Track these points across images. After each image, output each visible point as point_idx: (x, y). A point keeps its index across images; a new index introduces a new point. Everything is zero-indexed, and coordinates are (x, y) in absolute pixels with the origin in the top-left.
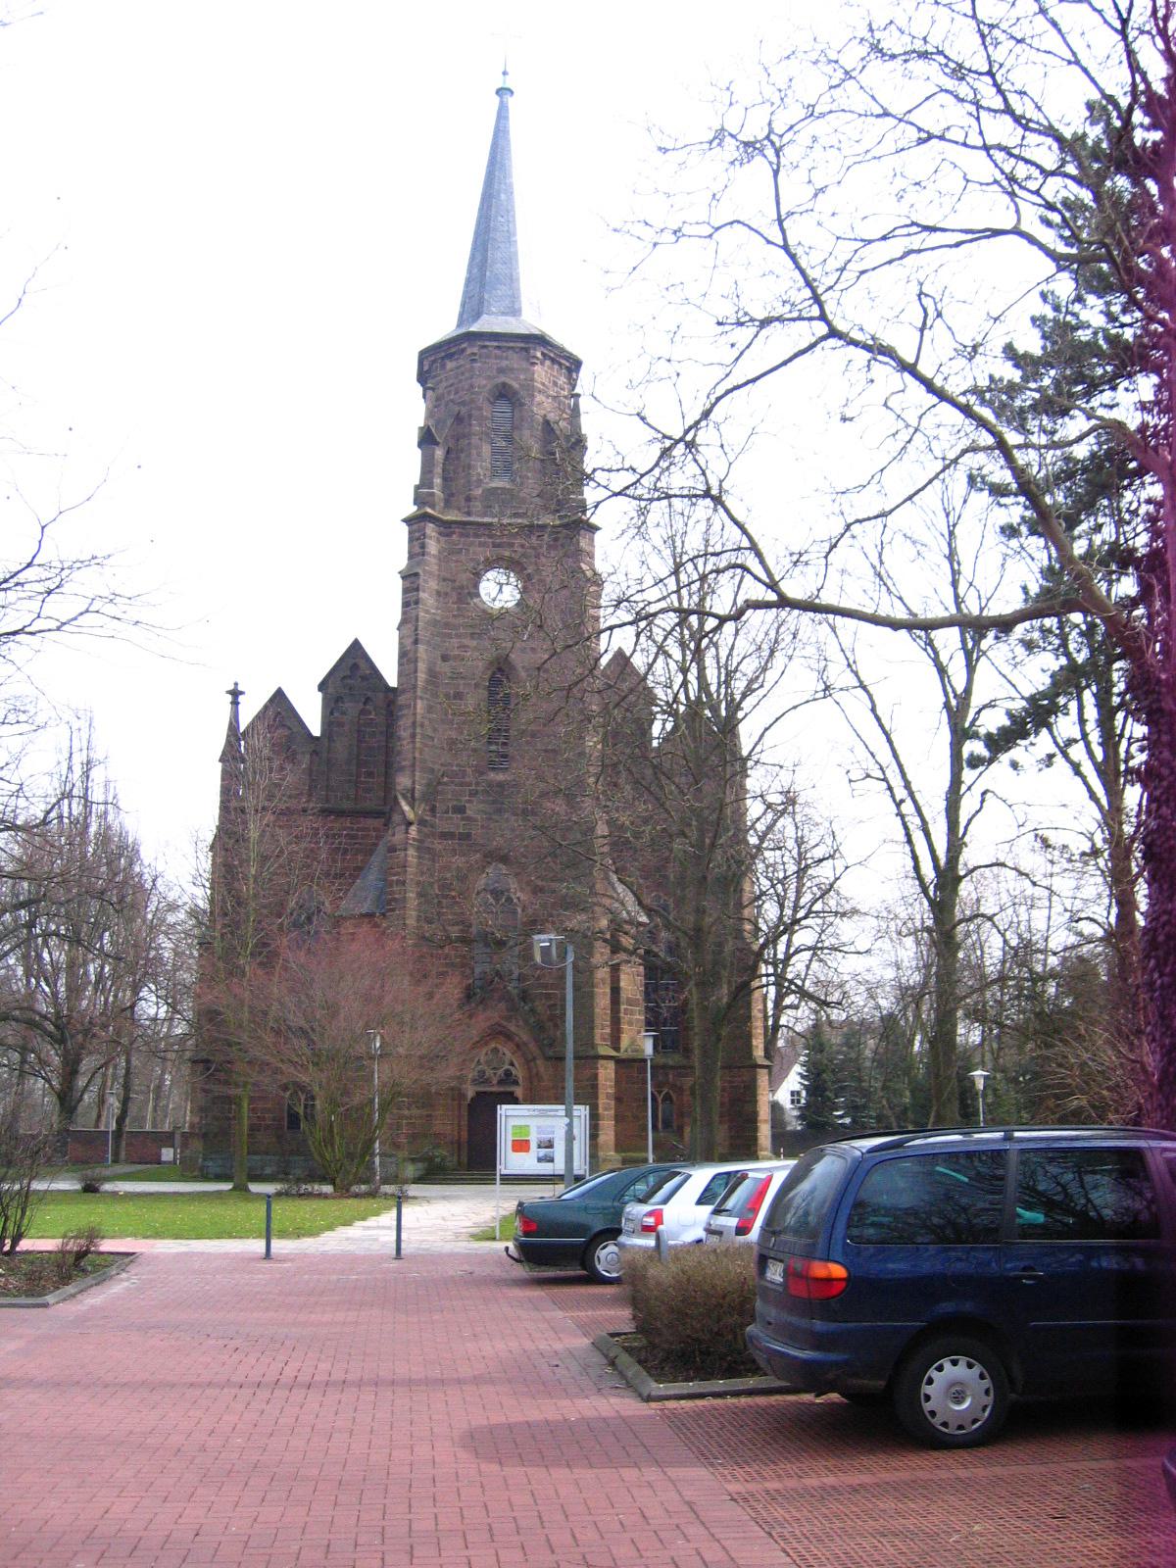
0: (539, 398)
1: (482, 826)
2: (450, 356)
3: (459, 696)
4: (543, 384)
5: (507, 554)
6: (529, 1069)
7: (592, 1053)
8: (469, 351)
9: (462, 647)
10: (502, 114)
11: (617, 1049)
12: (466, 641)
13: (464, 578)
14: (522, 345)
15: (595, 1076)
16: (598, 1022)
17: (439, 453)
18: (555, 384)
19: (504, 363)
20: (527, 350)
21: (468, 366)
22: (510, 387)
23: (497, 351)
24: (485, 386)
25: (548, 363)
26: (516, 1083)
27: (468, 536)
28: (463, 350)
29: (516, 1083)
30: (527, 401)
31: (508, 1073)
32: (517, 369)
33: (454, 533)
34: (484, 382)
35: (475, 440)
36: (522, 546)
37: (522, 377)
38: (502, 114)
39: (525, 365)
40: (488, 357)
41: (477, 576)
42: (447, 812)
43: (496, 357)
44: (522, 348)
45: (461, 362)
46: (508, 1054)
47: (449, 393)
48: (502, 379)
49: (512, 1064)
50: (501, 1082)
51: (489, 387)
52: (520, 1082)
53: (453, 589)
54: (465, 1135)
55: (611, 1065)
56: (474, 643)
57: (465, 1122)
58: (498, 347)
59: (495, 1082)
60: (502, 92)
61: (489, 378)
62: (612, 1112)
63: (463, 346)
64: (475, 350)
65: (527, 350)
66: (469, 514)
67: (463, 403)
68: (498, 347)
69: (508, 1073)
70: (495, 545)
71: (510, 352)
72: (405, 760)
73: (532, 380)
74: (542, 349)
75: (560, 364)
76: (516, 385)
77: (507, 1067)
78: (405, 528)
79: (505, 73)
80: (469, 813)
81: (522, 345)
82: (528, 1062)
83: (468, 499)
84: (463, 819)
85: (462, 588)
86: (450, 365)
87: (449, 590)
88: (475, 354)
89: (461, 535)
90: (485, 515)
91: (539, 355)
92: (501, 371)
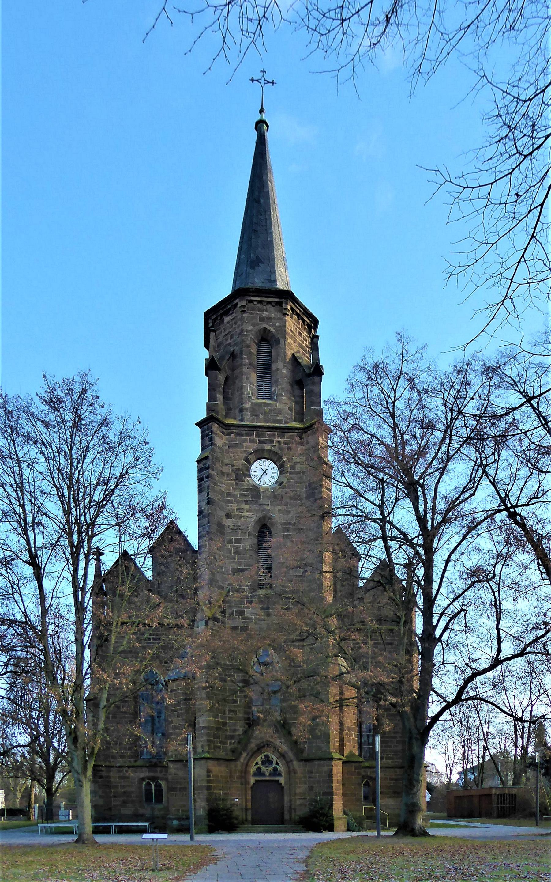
0: (289, 340)
1: (256, 623)
2: (227, 313)
3: (238, 541)
4: (291, 331)
5: (269, 447)
6: (289, 768)
7: (329, 757)
8: (240, 305)
9: (239, 509)
10: (261, 142)
11: (343, 755)
12: (243, 506)
13: (240, 463)
14: (277, 300)
15: (331, 770)
16: (332, 738)
17: (221, 378)
18: (300, 334)
19: (265, 314)
20: (280, 304)
21: (239, 317)
22: (269, 331)
23: (259, 305)
24: (251, 331)
25: (295, 317)
26: (280, 775)
27: (241, 435)
28: (237, 304)
29: (280, 775)
30: (282, 341)
31: (275, 769)
32: (274, 318)
33: (232, 433)
34: (250, 328)
35: (245, 369)
36: (279, 442)
37: (277, 324)
38: (261, 142)
39: (279, 315)
40: (253, 309)
41: (249, 463)
42: (232, 614)
43: (259, 310)
44: (277, 303)
45: (234, 315)
46: (275, 758)
47: (226, 340)
48: (264, 325)
49: (277, 764)
50: (270, 775)
52: (283, 774)
53: (232, 470)
54: (249, 805)
55: (340, 763)
56: (247, 507)
57: (249, 797)
58: (260, 302)
59: (267, 774)
60: (260, 126)
61: (254, 325)
62: (341, 791)
63: (235, 302)
64: (244, 303)
65: (280, 304)
66: (242, 420)
67: (236, 344)
68: (260, 302)
69: (275, 769)
70: (260, 442)
71: (269, 306)
72: (204, 580)
73: (285, 326)
74: (292, 304)
75: (303, 320)
76: (272, 330)
77: (274, 765)
78: (198, 430)
79: (262, 111)
80: (247, 615)
81: (277, 300)
82: (287, 763)
83: (241, 410)
84: (243, 618)
85: (238, 470)
86: (227, 319)
87: (230, 471)
88: (244, 306)
89: (237, 434)
90: (253, 420)
91: (289, 308)
92: (262, 319)
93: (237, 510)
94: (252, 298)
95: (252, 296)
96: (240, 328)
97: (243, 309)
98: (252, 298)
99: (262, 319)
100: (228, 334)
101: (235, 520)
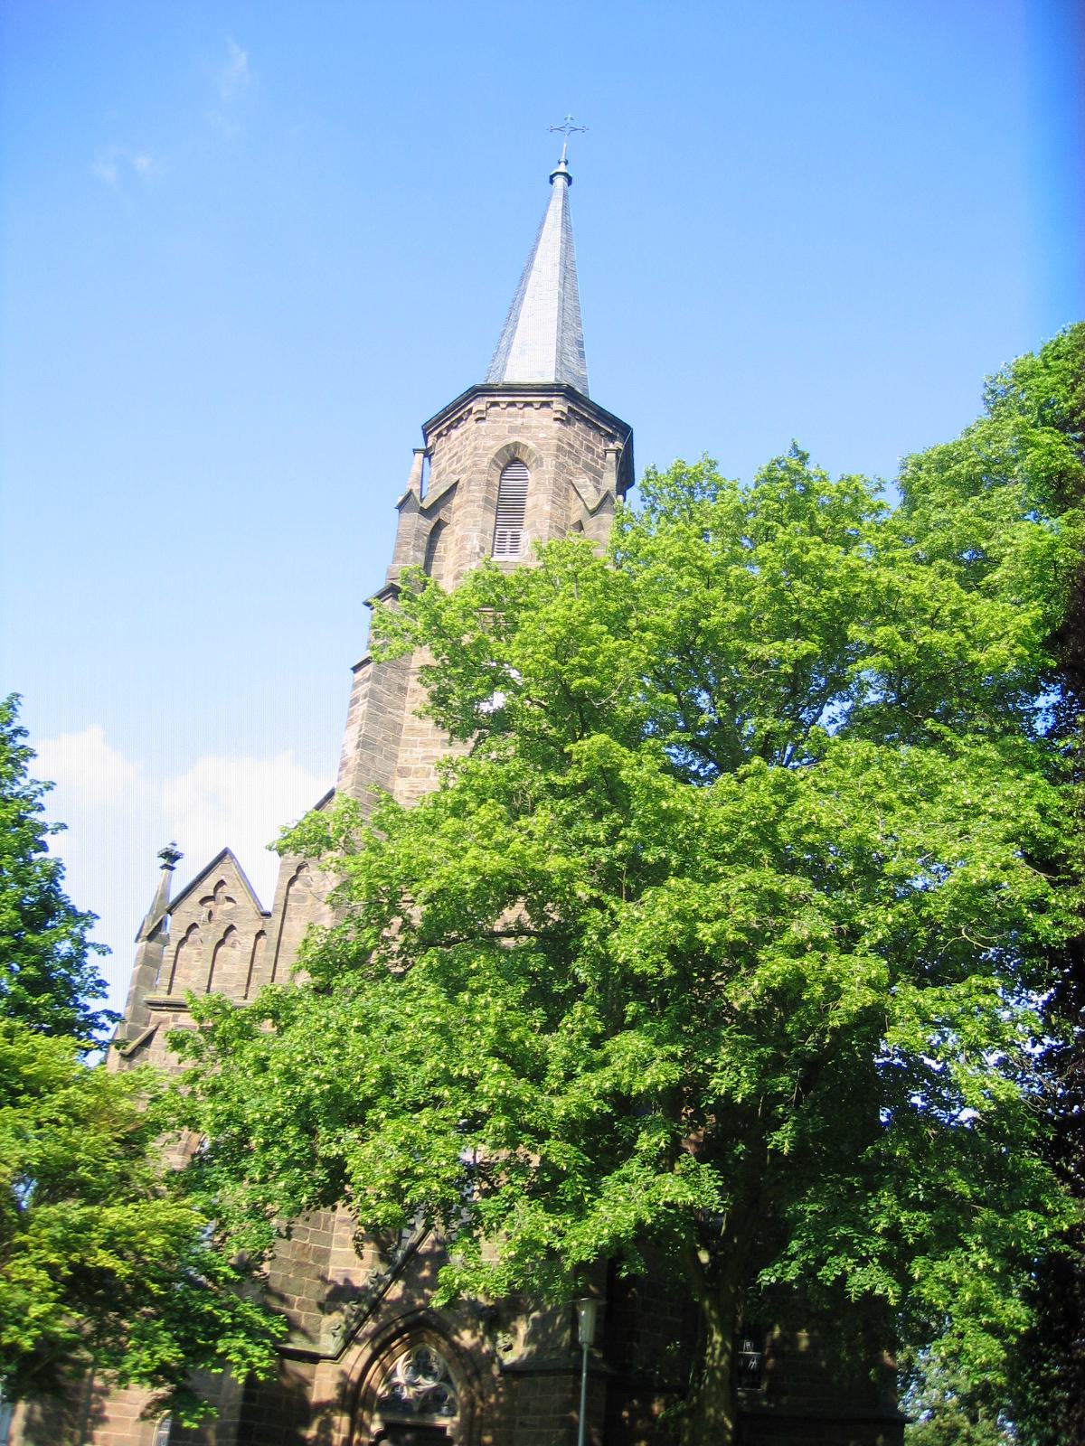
8: (474, 411)
19: (519, 421)
21: (474, 428)
24: (491, 448)
28: (470, 411)
37: (541, 435)
40: (499, 415)
43: (510, 415)
51: (495, 450)
61: (498, 438)
76: (531, 445)
92: (513, 430)
93: (423, 759)
94: (497, 399)
95: (499, 396)
96: (473, 444)
97: (479, 416)
98: (497, 399)
99: (513, 430)
100: (455, 455)
101: (415, 780)
